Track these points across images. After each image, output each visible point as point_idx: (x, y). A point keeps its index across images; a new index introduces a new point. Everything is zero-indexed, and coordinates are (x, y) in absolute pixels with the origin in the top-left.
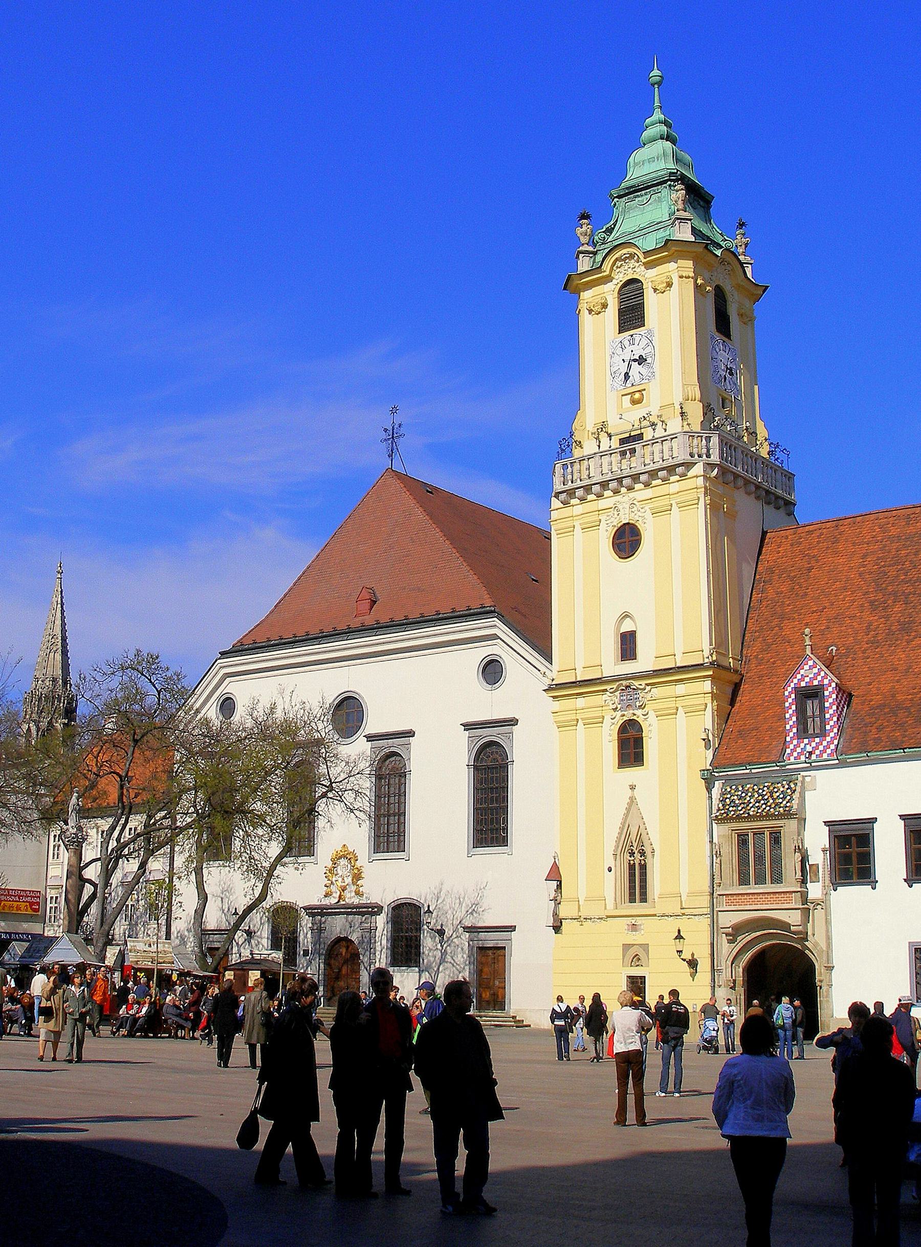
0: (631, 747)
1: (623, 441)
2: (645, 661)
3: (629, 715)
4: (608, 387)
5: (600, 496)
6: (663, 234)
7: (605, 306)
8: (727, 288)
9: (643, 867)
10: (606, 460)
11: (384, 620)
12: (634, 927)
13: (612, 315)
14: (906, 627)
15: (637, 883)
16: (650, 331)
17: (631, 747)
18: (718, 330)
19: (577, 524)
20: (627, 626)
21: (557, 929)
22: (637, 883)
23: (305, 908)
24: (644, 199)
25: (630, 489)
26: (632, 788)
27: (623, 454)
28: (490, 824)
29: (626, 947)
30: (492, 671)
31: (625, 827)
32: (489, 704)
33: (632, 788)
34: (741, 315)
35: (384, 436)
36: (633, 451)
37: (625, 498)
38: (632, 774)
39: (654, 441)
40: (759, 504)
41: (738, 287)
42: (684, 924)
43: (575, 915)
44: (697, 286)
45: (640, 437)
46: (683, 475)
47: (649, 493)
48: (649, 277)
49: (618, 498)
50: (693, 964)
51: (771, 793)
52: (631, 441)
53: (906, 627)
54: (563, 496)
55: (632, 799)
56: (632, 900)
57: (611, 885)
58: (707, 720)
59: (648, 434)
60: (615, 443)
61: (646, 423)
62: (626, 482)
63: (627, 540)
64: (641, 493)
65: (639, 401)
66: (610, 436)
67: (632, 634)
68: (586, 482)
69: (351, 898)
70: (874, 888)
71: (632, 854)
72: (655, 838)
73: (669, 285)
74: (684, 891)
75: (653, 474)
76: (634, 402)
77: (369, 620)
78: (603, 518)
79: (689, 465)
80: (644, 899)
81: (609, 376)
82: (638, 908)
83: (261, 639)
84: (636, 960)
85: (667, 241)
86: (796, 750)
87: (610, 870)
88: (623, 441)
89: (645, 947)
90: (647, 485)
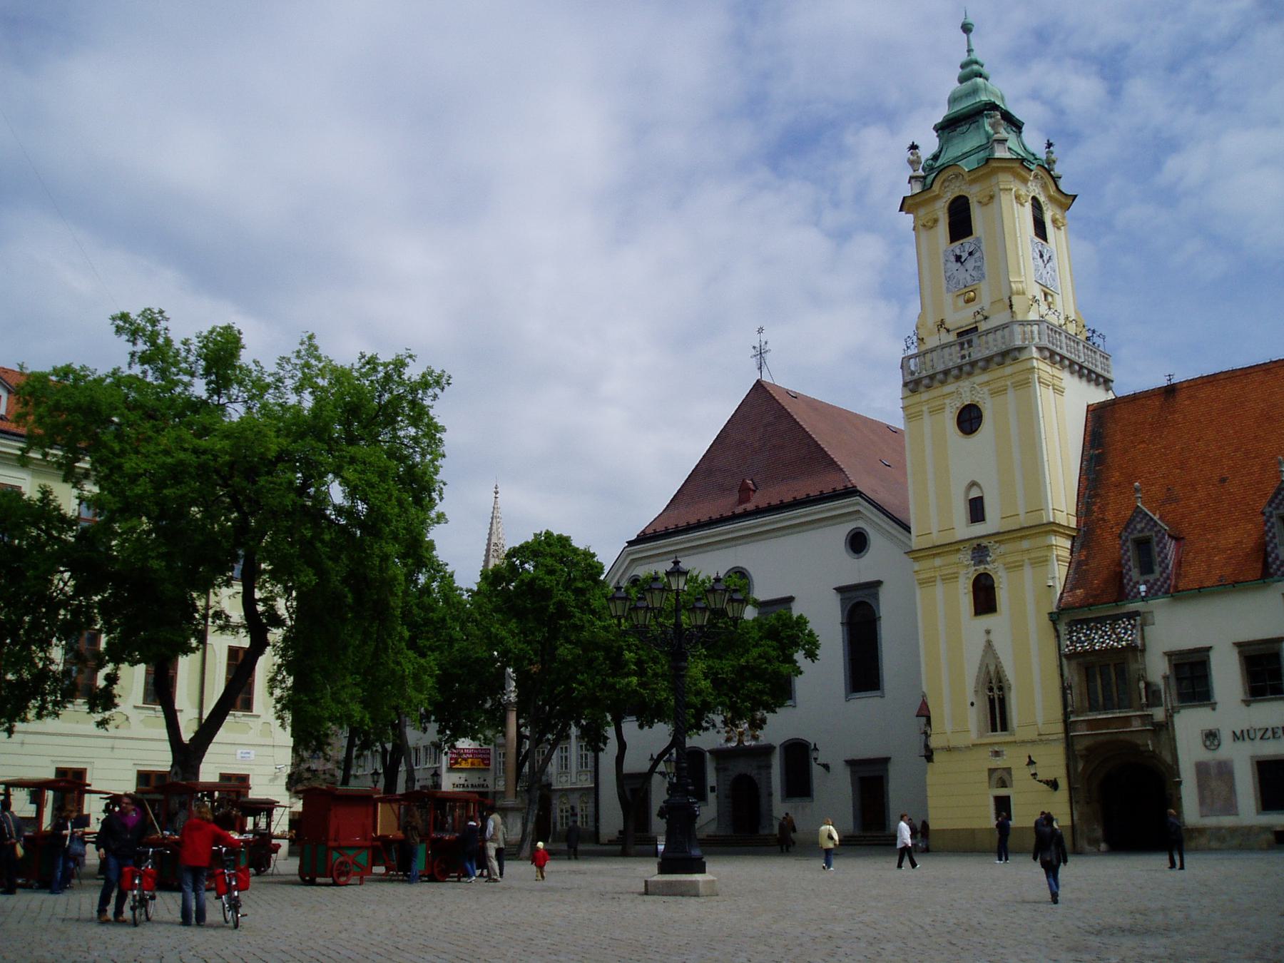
0: (984, 598)
1: (960, 335)
3: (981, 568)
4: (944, 289)
5: (943, 383)
6: (982, 155)
7: (936, 221)
8: (1042, 199)
9: (1002, 701)
10: (947, 351)
11: (763, 505)
12: (997, 754)
13: (943, 229)
15: (998, 715)
16: (978, 239)
17: (984, 598)
18: (1037, 234)
19: (925, 408)
20: (974, 494)
21: (929, 755)
22: (998, 715)
23: (711, 752)
24: (964, 128)
25: (970, 374)
26: (988, 632)
27: (962, 345)
28: (864, 672)
29: (992, 771)
30: (858, 543)
31: (984, 666)
32: (857, 571)
33: (988, 632)
34: (1054, 221)
35: (754, 352)
36: (970, 342)
37: (965, 385)
38: (987, 621)
39: (987, 332)
40: (1084, 383)
41: (1050, 198)
43: (945, 744)
44: (1017, 197)
45: (976, 328)
46: (1015, 359)
47: (985, 377)
48: (974, 193)
49: (961, 383)
50: (1054, 785)
51: (1113, 629)
52: (967, 335)
54: (911, 386)
55: (989, 644)
56: (994, 729)
57: (973, 720)
59: (983, 327)
60: (952, 337)
61: (979, 317)
62: (967, 368)
63: (969, 419)
65: (973, 300)
66: (948, 331)
67: (981, 498)
68: (931, 372)
69: (748, 743)
70: (1214, 709)
71: (991, 689)
72: (1010, 674)
73: (992, 197)
74: (1040, 720)
75: (988, 360)
76: (968, 301)
77: (750, 506)
78: (947, 401)
80: (1004, 728)
81: (944, 282)
82: (999, 737)
83: (660, 528)
84: (1003, 784)
85: (988, 160)
87: (972, 704)
88: (960, 335)
89: (1008, 770)
90: (984, 369)
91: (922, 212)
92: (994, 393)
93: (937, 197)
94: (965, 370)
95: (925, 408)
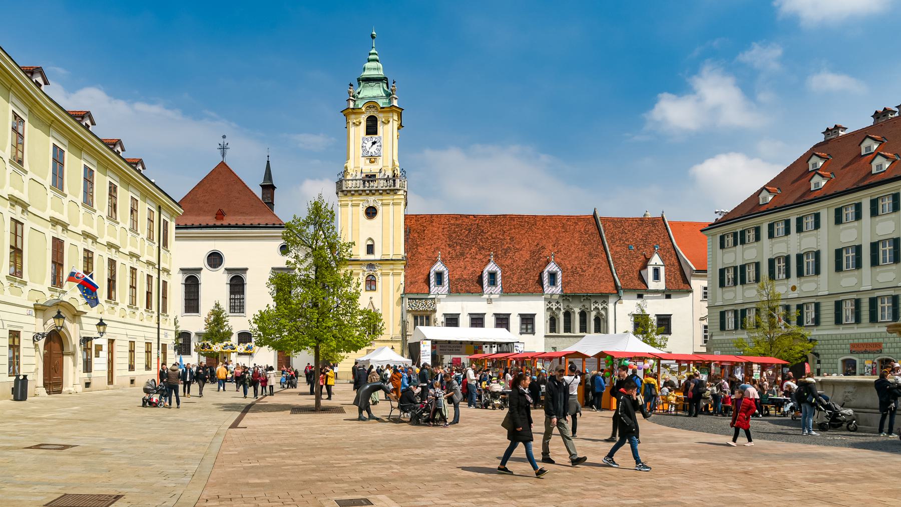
2: (377, 255)
5: (360, 195)
13: (363, 127)
14: (462, 254)
20: (370, 243)
24: (373, 84)
25: (374, 194)
38: (371, 294)
42: (394, 345)
47: (380, 197)
48: (381, 117)
52: (371, 177)
53: (462, 254)
58: (402, 279)
63: (371, 212)
64: (377, 197)
79: (399, 190)
86: (434, 289)
90: (381, 194)
91: (353, 116)
92: (383, 204)
93: (363, 113)
94: (372, 192)
95: (350, 203)
